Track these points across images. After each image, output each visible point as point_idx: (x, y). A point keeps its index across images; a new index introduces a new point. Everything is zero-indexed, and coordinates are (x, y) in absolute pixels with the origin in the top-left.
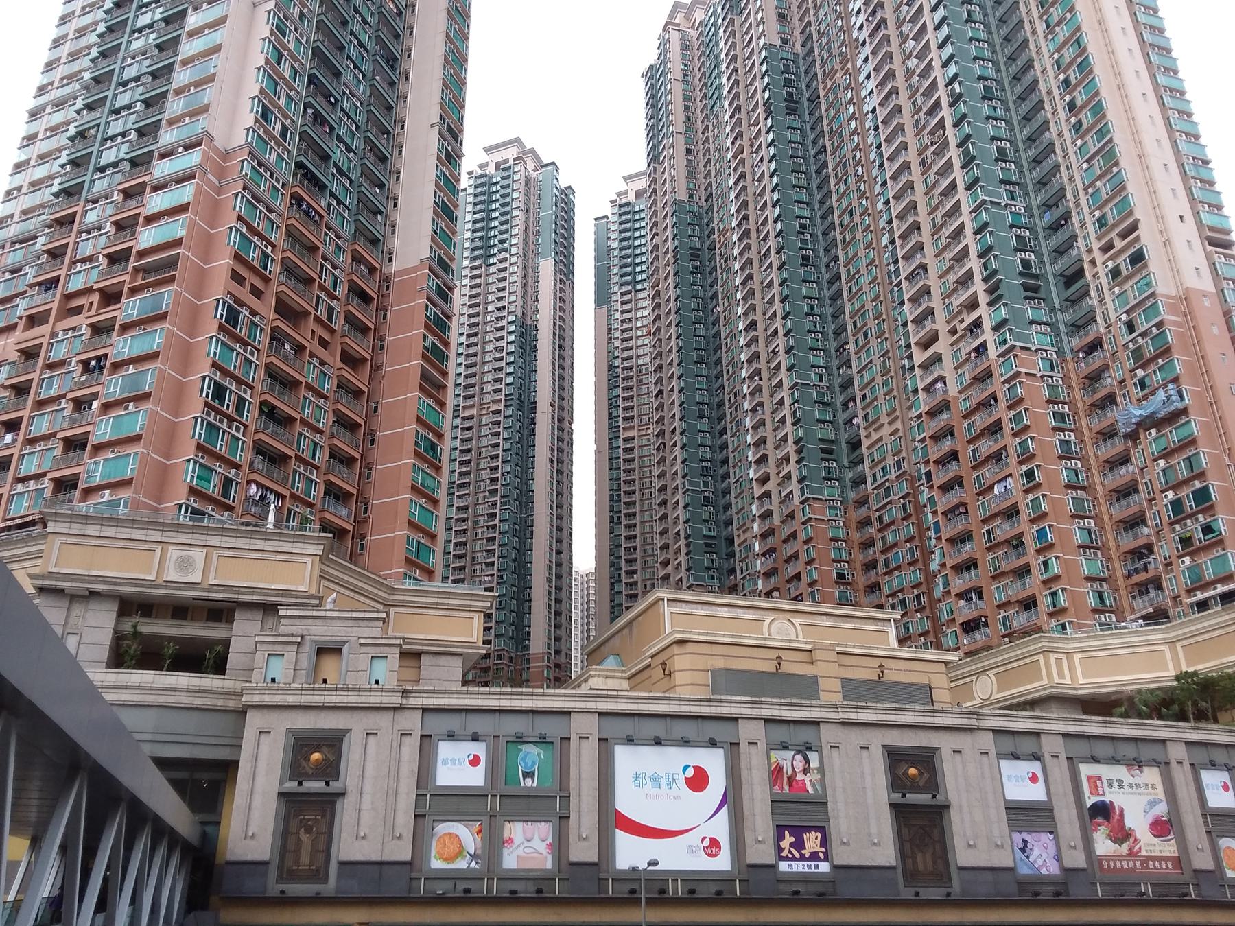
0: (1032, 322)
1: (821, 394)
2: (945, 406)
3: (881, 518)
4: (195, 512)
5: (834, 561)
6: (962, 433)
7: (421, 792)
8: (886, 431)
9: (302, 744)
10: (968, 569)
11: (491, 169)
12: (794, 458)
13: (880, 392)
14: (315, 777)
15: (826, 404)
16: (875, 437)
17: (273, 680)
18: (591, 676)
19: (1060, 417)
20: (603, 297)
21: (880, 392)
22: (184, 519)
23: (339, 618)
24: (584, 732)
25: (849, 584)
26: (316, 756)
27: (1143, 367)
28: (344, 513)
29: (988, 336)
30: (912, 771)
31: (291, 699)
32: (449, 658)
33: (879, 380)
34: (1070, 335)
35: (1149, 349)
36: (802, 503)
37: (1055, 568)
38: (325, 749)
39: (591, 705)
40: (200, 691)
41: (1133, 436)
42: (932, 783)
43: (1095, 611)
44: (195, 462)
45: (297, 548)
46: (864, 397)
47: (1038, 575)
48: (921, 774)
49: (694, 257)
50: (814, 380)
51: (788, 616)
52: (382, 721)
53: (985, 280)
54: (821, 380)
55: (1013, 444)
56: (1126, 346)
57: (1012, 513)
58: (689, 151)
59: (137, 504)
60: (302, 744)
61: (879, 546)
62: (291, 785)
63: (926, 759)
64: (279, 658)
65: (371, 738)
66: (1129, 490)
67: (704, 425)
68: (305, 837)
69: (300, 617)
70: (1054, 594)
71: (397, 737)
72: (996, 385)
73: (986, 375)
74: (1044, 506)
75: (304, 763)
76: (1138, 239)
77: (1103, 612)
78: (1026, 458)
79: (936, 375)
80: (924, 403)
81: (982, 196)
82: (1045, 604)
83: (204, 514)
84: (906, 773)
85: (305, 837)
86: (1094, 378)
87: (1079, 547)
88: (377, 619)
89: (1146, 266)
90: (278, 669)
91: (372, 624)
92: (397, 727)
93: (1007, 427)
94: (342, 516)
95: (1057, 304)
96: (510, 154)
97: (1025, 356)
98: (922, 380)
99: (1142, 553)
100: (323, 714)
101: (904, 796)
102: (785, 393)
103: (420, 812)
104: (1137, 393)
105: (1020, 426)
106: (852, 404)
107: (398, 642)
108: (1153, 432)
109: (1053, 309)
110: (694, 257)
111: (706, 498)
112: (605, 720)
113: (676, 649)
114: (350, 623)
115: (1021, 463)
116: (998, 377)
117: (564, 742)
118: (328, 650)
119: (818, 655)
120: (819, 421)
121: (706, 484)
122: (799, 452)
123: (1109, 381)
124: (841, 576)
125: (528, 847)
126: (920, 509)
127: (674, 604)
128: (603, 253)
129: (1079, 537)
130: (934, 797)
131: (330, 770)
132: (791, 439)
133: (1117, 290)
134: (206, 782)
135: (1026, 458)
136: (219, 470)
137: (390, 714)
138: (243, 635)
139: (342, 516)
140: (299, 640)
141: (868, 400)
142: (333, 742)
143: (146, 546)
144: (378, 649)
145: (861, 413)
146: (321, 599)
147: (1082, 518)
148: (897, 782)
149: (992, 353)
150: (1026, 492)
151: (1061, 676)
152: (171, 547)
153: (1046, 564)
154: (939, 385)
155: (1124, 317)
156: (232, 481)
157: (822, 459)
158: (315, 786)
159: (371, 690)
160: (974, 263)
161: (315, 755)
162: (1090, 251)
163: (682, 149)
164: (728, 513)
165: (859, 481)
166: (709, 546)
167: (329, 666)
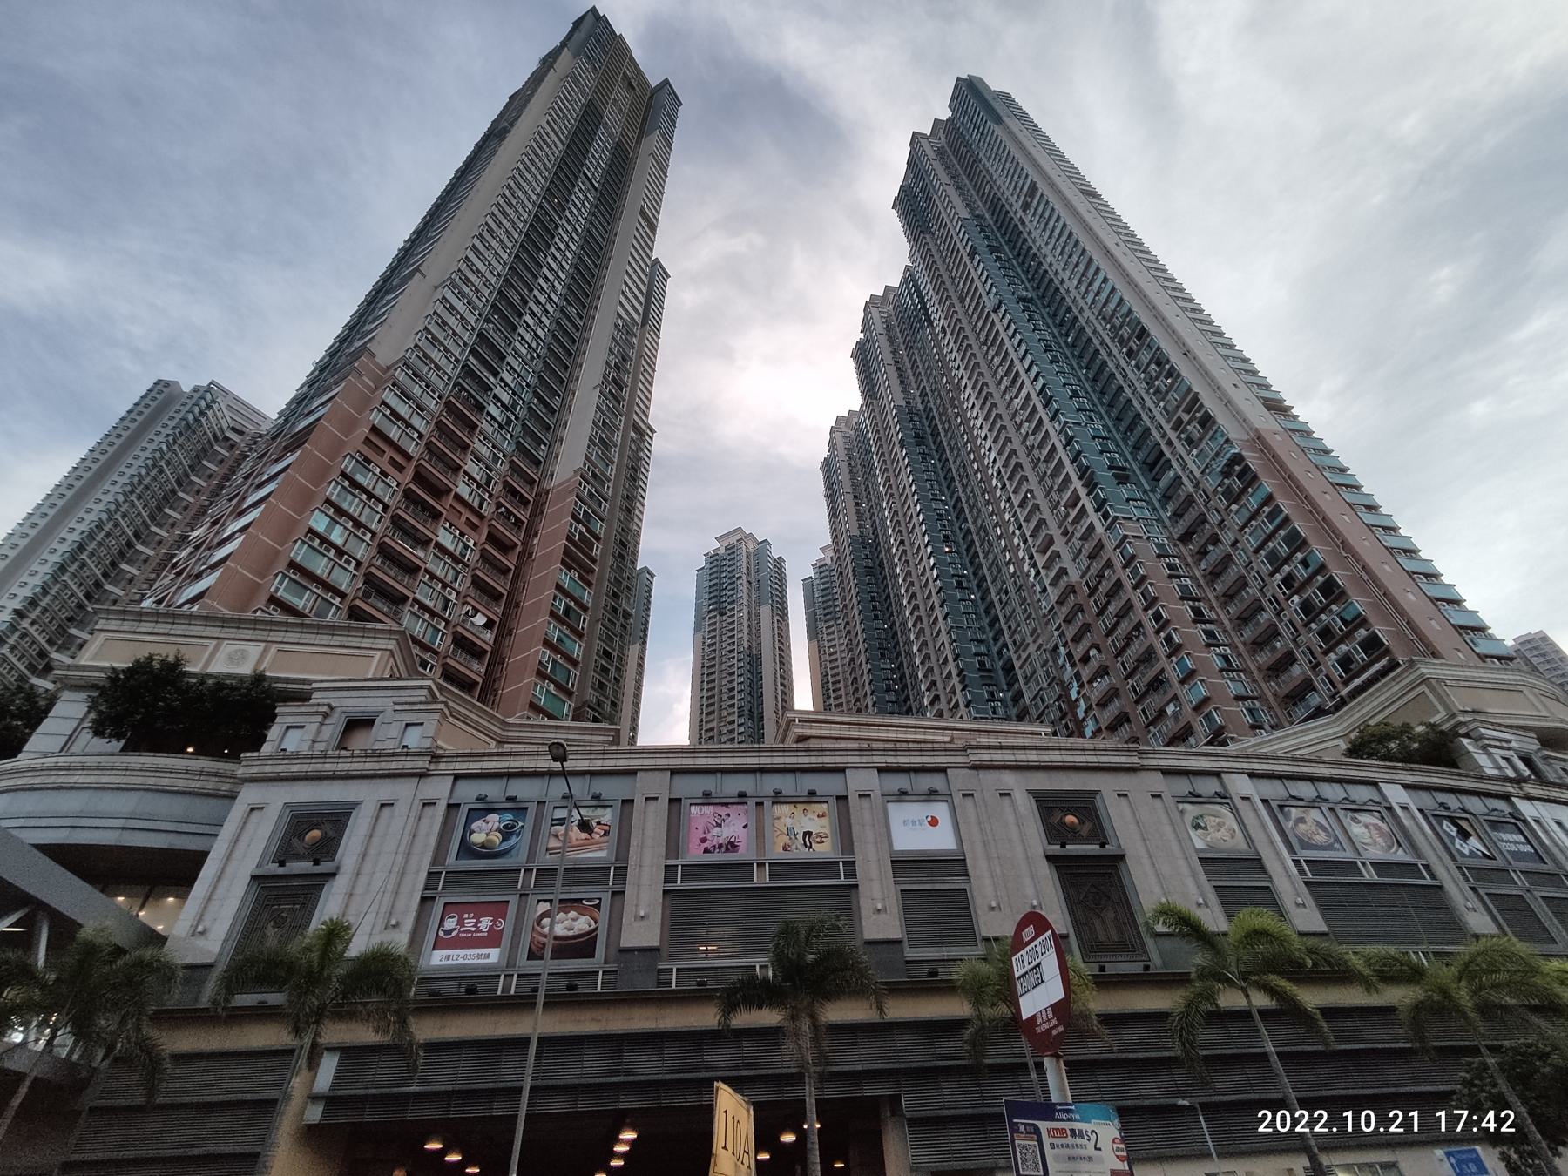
8: (1032, 648)
11: (722, 551)
12: (958, 687)
13: (1021, 618)
15: (980, 642)
16: (1024, 656)
20: (813, 633)
21: (1021, 618)
23: (378, 688)
24: (652, 792)
26: (316, 833)
27: (1235, 502)
28: (476, 666)
30: (1070, 819)
33: (1019, 610)
34: (1164, 508)
38: (328, 826)
42: (1099, 833)
44: (285, 576)
45: (366, 643)
48: (1081, 822)
52: (403, 791)
53: (1080, 478)
60: (300, 820)
62: (274, 869)
63: (1085, 804)
70: (1209, 717)
71: (417, 805)
73: (1100, 546)
74: (1176, 639)
75: (295, 841)
76: (1202, 405)
78: (1151, 602)
80: (1053, 594)
81: (1062, 419)
84: (1063, 824)
87: (1221, 670)
88: (421, 687)
89: (1215, 422)
92: (420, 796)
93: (1128, 584)
94: (476, 670)
95: (1147, 487)
96: (733, 540)
97: (1128, 524)
101: (1063, 846)
102: (944, 637)
103: (429, 894)
109: (1145, 491)
112: (677, 778)
114: (390, 693)
115: (1146, 609)
116: (1109, 546)
117: (627, 806)
118: (358, 723)
126: (1073, 705)
128: (810, 602)
129: (1219, 663)
130: (1103, 845)
131: (327, 848)
132: (954, 674)
133: (1195, 452)
135: (1151, 602)
139: (476, 670)
140: (325, 709)
145: (1009, 642)
148: (1055, 832)
149: (1100, 529)
150: (1157, 632)
160: (1070, 469)
162: (1164, 435)
165: (1018, 696)
167: (360, 741)
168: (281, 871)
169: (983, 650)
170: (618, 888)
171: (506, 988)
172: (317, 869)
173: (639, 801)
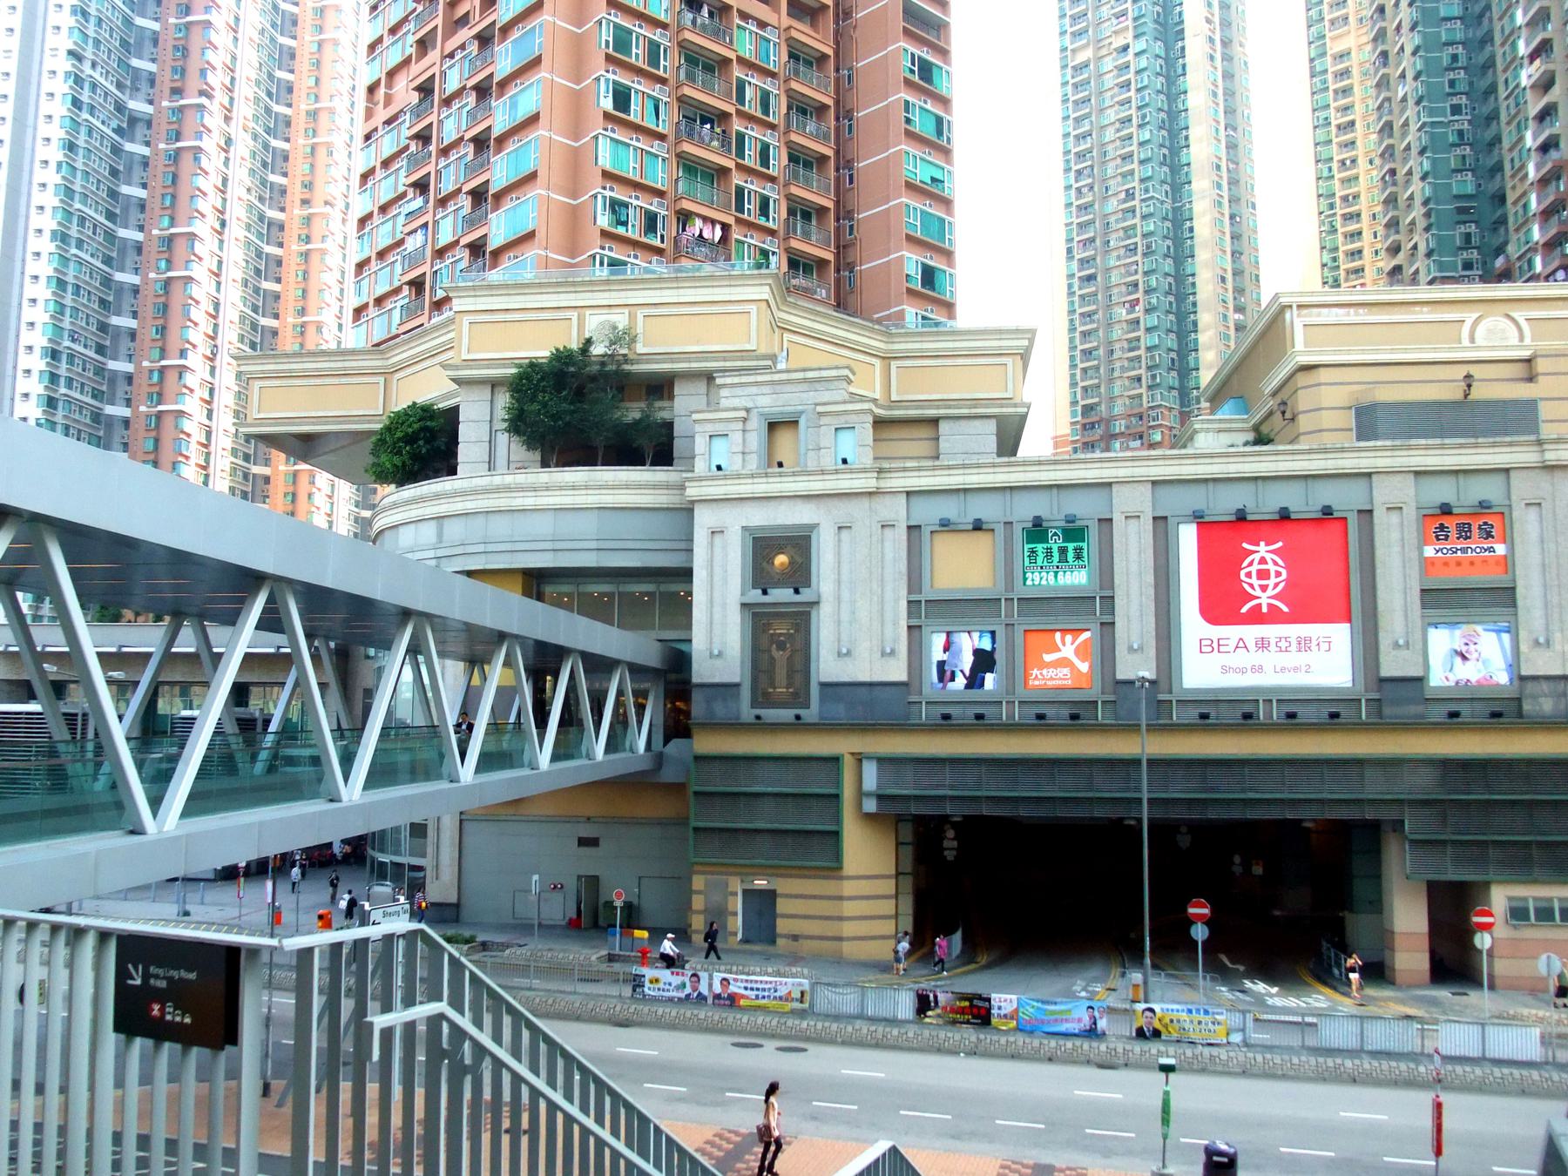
4: (613, 263)
7: (914, 597)
9: (763, 546)
14: (779, 584)
17: (719, 468)
18: (1195, 432)
22: (603, 273)
24: (1132, 509)
32: (977, 423)
40: (627, 486)
59: (546, 263)
60: (763, 546)
62: (755, 596)
64: (723, 440)
65: (845, 533)
68: (777, 654)
69: (742, 385)
83: (625, 264)
85: (777, 654)
90: (722, 452)
91: (833, 385)
103: (915, 622)
107: (866, 406)
112: (1161, 491)
114: (805, 386)
125: (1063, 664)
127: (1305, 312)
131: (800, 575)
134: (662, 590)
136: (635, 202)
137: (865, 502)
140: (743, 414)
142: (799, 543)
143: (561, 314)
144: (843, 419)
146: (773, 358)
152: (588, 312)
156: (656, 215)
158: (782, 595)
159: (837, 472)
161: (780, 558)
168: (766, 599)
170: (1107, 619)
171: (1011, 715)
172: (798, 598)
173: (1118, 518)
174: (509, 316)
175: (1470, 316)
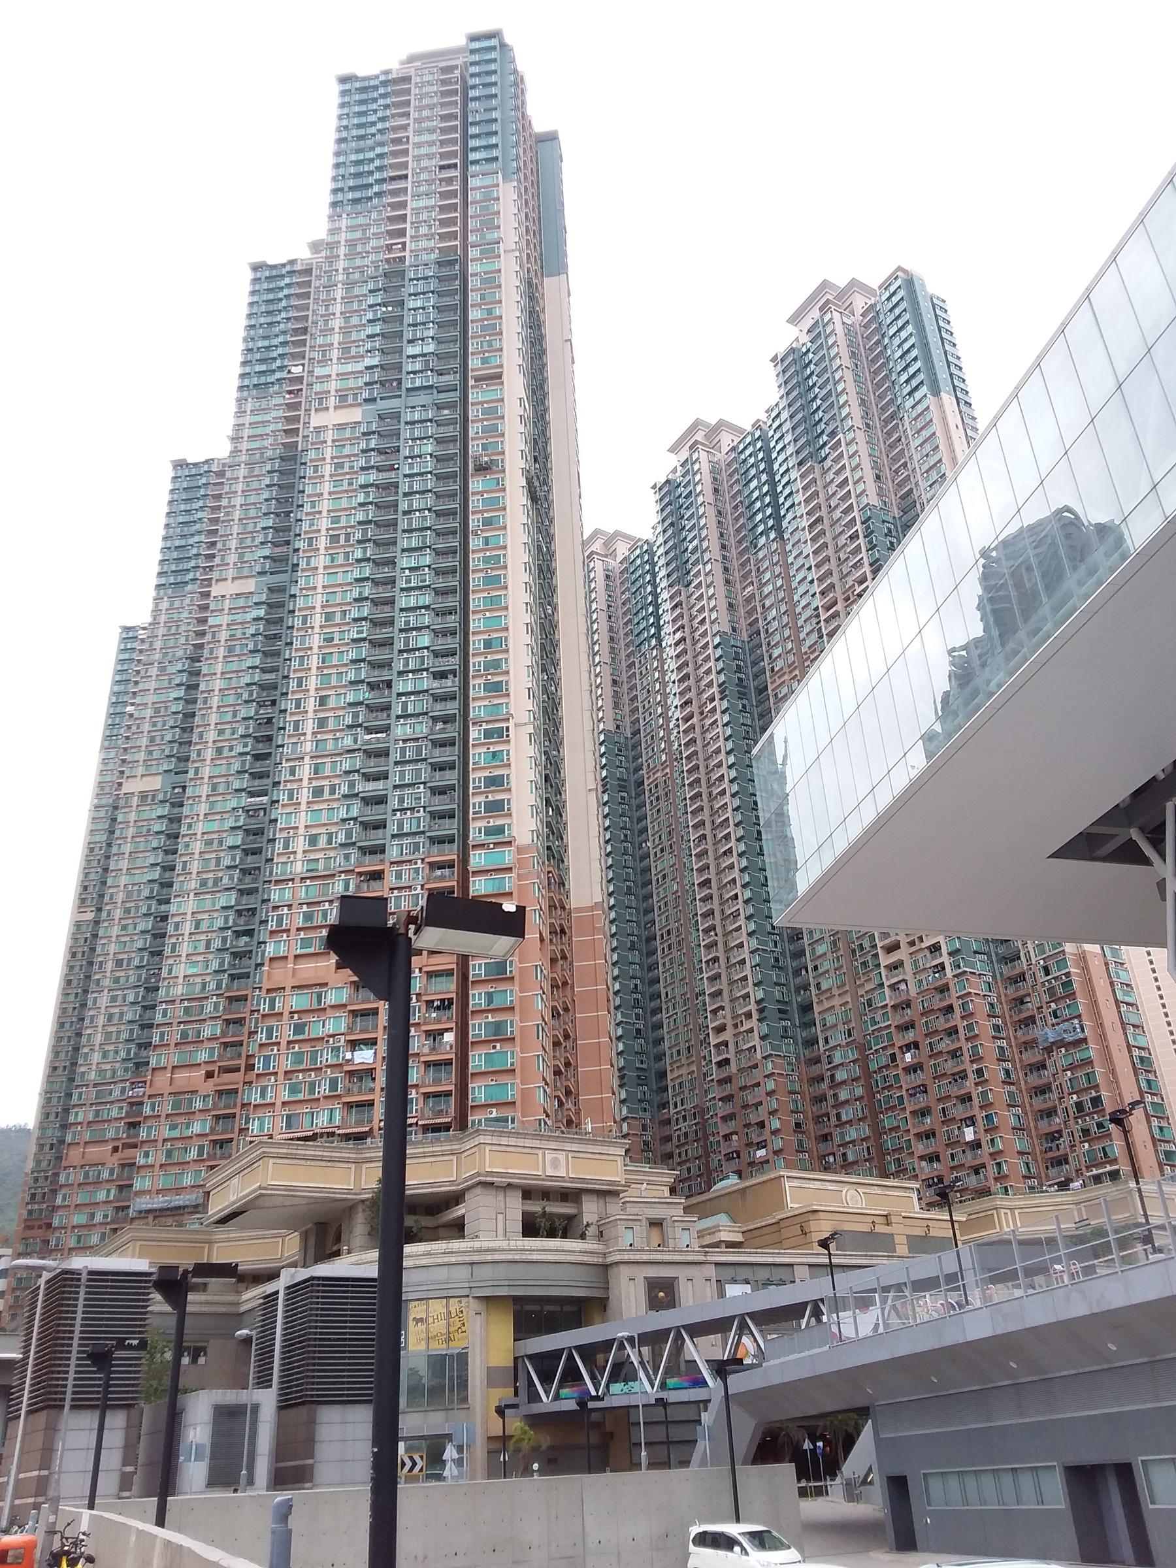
0: (975, 952)
1: (777, 960)
2: (908, 1004)
3: (832, 1076)
5: (792, 1112)
6: (920, 1027)
8: (836, 1002)
10: (928, 1138)
16: (827, 1005)
19: (997, 1028)
25: (804, 1132)
29: (945, 959)
31: (645, 1257)
35: (1060, 991)
36: (765, 1058)
37: (1000, 1145)
39: (804, 1260)
41: (1049, 1050)
43: (1024, 1177)
46: (816, 968)
47: (986, 1149)
49: (622, 788)
50: (771, 944)
51: (855, 1187)
54: (776, 946)
55: (966, 1047)
56: (1043, 984)
57: (967, 1098)
58: (615, 682)
61: (831, 1101)
66: (1043, 1090)
67: (634, 956)
70: (999, 1164)
72: (953, 998)
77: (1029, 1178)
79: (901, 978)
80: (889, 998)
82: (991, 1171)
86: (1021, 1001)
87: (1014, 1128)
98: (887, 979)
99: (1053, 1136)
100: (662, 1267)
104: (1051, 1020)
105: (972, 1034)
106: (804, 972)
108: (1063, 1050)
110: (622, 788)
111: (638, 1031)
113: (811, 1217)
115: (972, 1062)
116: (955, 992)
119: (893, 1219)
120: (776, 984)
121: (638, 1017)
122: (761, 1011)
123: (1031, 1007)
124: (798, 1125)
129: (1013, 1122)
138: (590, 1211)
141: (820, 971)
147: (1014, 1106)
149: (949, 973)
150: (977, 1084)
151: (1008, 1226)
153: (992, 1140)
154: (903, 986)
155: (1042, 962)
157: (781, 1019)
163: (608, 680)
164: (660, 1048)
166: (641, 1080)
169: (783, 981)
174: (509, 1149)
175: (847, 1187)
